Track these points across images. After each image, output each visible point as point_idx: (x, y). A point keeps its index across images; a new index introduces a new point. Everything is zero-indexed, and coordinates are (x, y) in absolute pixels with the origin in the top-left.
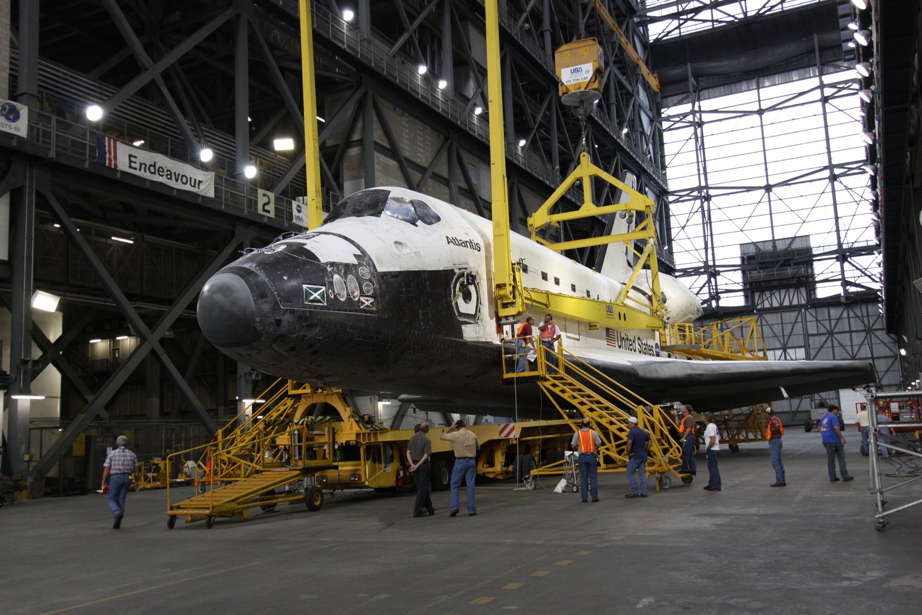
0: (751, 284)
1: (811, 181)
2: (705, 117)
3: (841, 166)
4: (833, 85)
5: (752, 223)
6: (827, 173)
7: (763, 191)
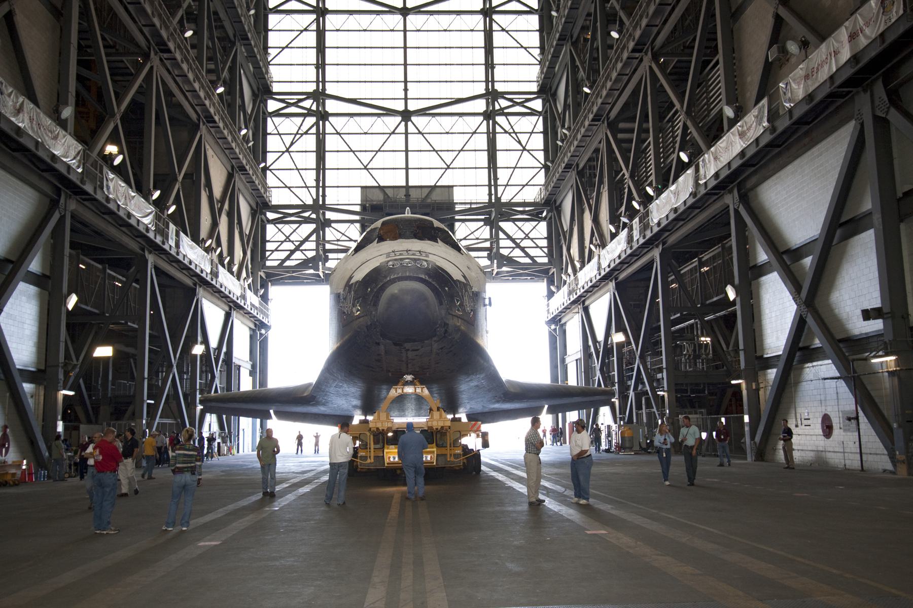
1: (461, 115)
5: (381, 160)
7: (399, 119)
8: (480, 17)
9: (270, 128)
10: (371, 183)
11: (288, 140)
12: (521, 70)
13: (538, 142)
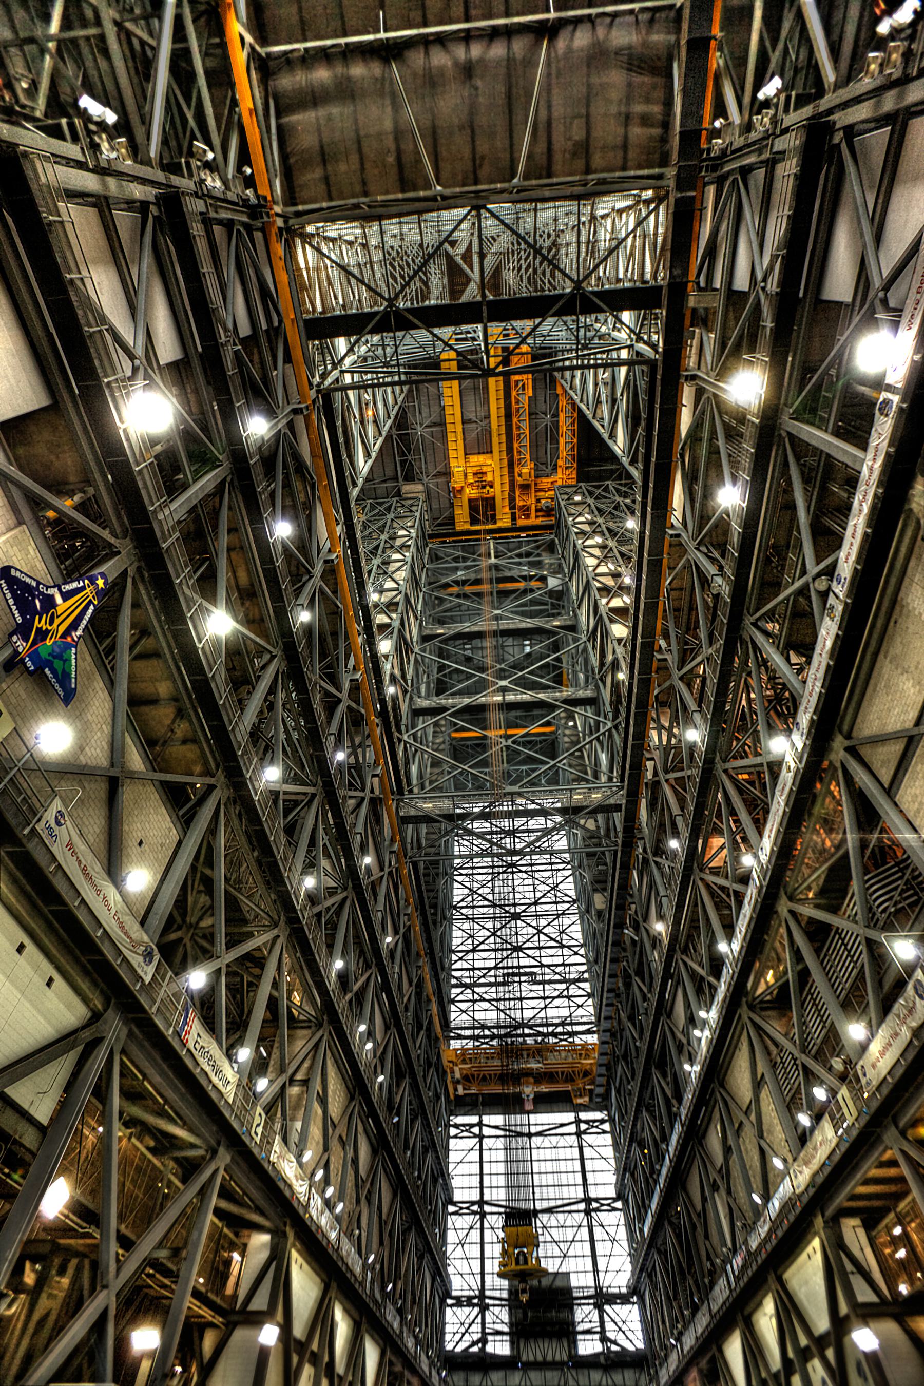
2: (486, 1131)
3: (596, 1200)
4: (587, 1122)
6: (582, 1206)
8: (575, 1137)
9: (450, 1225)
11: (462, 1234)
12: (604, 1182)
13: (622, 1234)
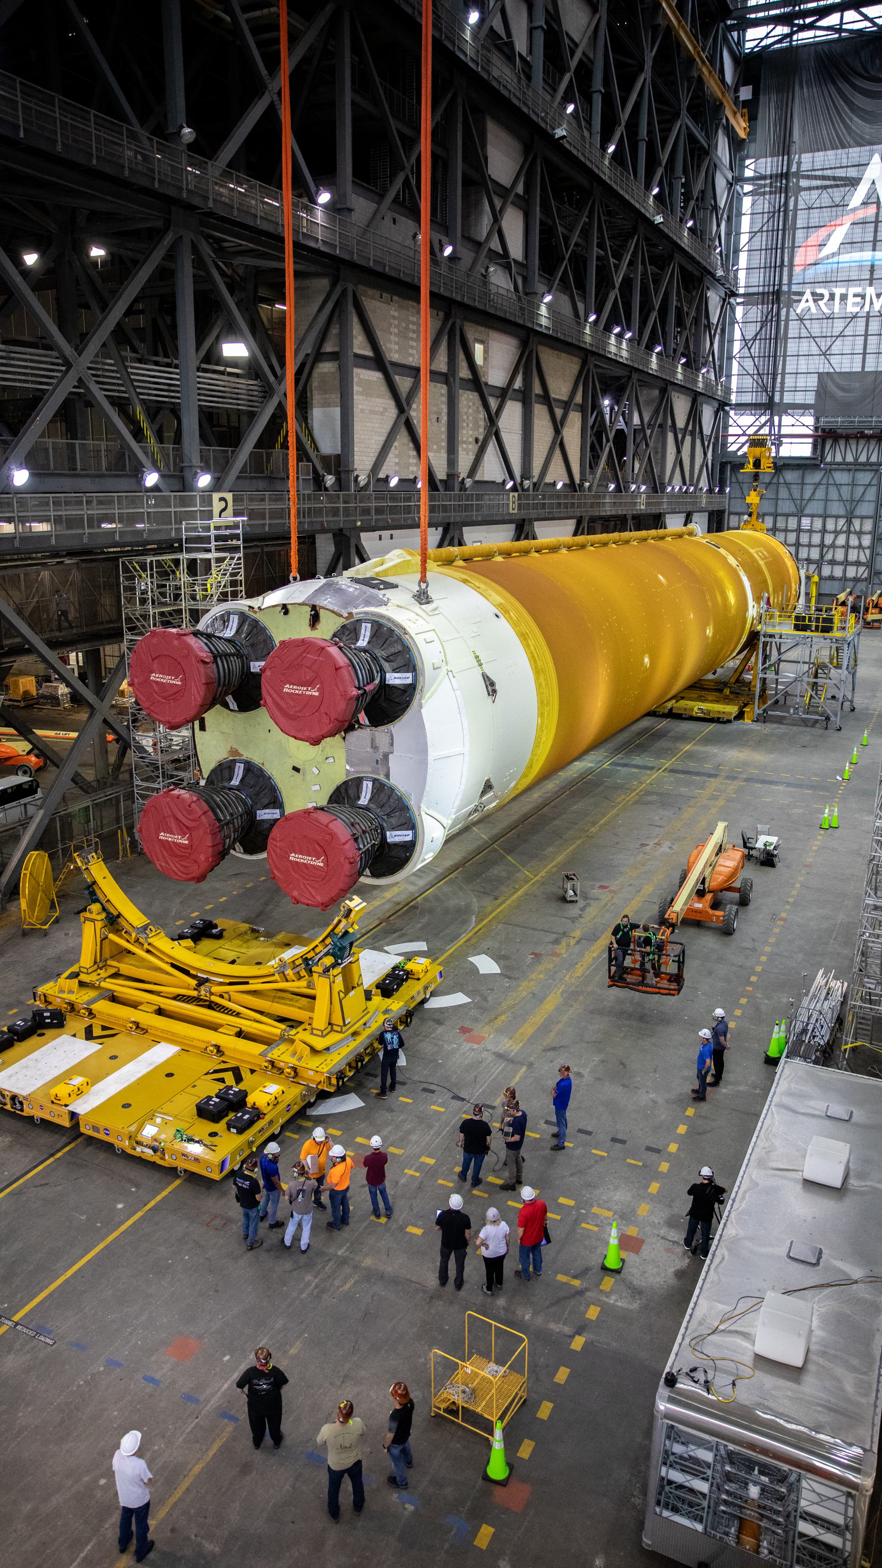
0: (823, 430)
10: (828, 369)
